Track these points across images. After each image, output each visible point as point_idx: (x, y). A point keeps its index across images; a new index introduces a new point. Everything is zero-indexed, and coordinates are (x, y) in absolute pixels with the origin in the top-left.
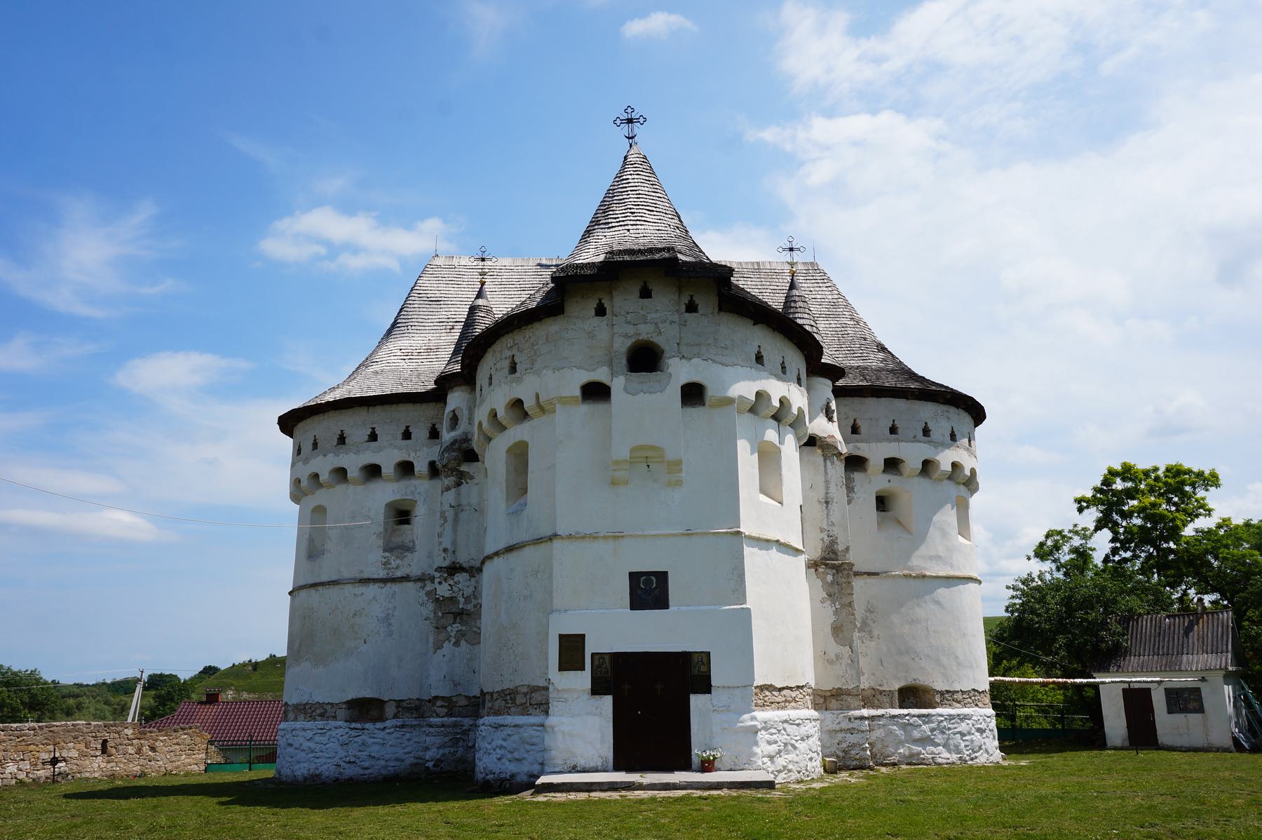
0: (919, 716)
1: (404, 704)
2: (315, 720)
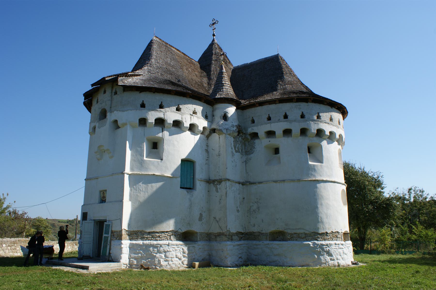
0: (278, 245)
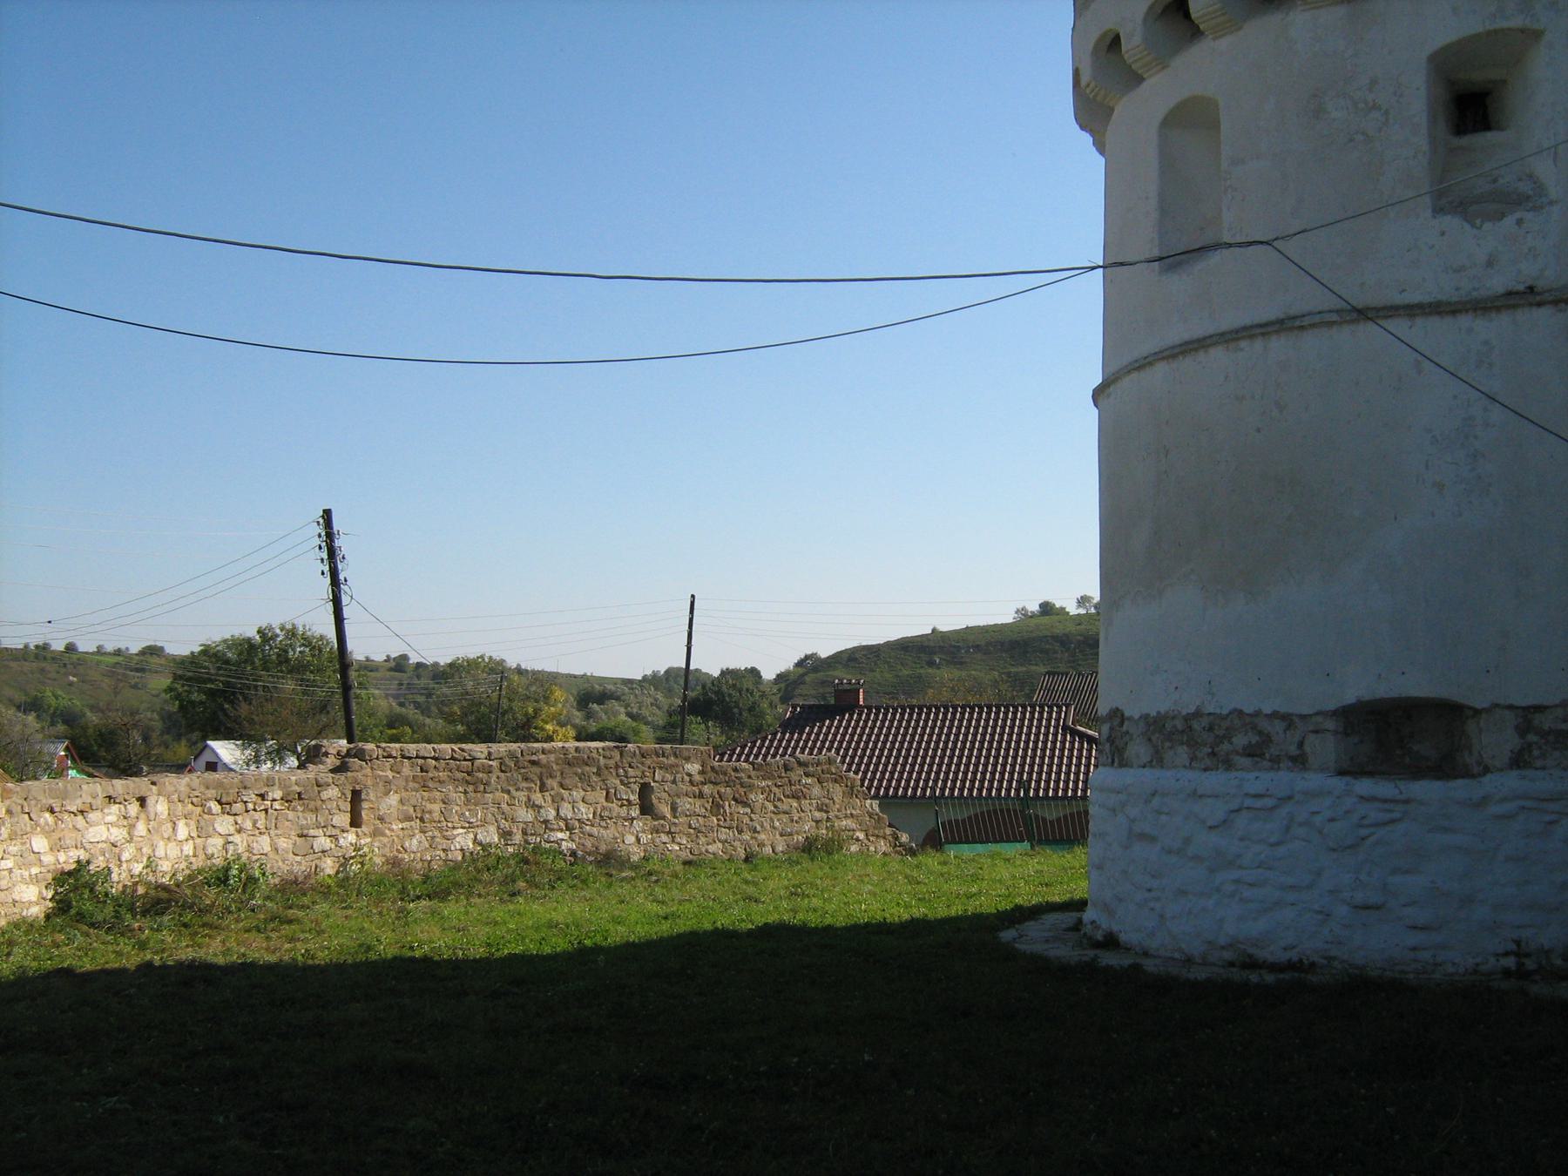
1: (1546, 722)
2: (1228, 765)
